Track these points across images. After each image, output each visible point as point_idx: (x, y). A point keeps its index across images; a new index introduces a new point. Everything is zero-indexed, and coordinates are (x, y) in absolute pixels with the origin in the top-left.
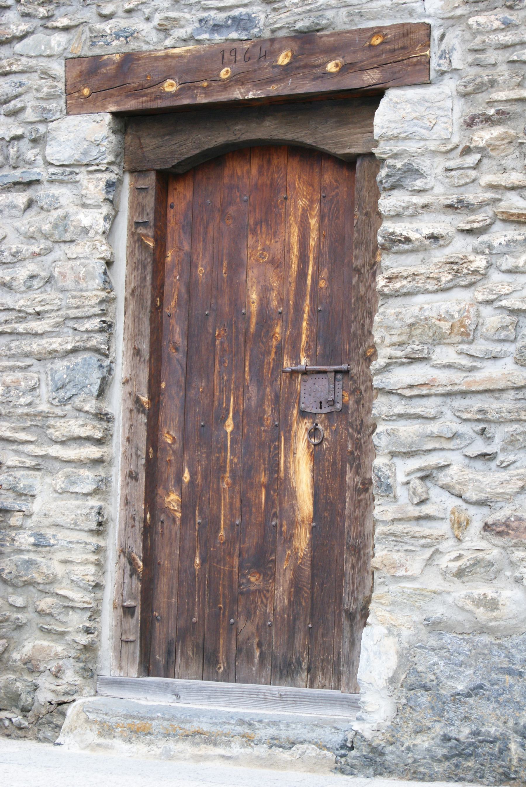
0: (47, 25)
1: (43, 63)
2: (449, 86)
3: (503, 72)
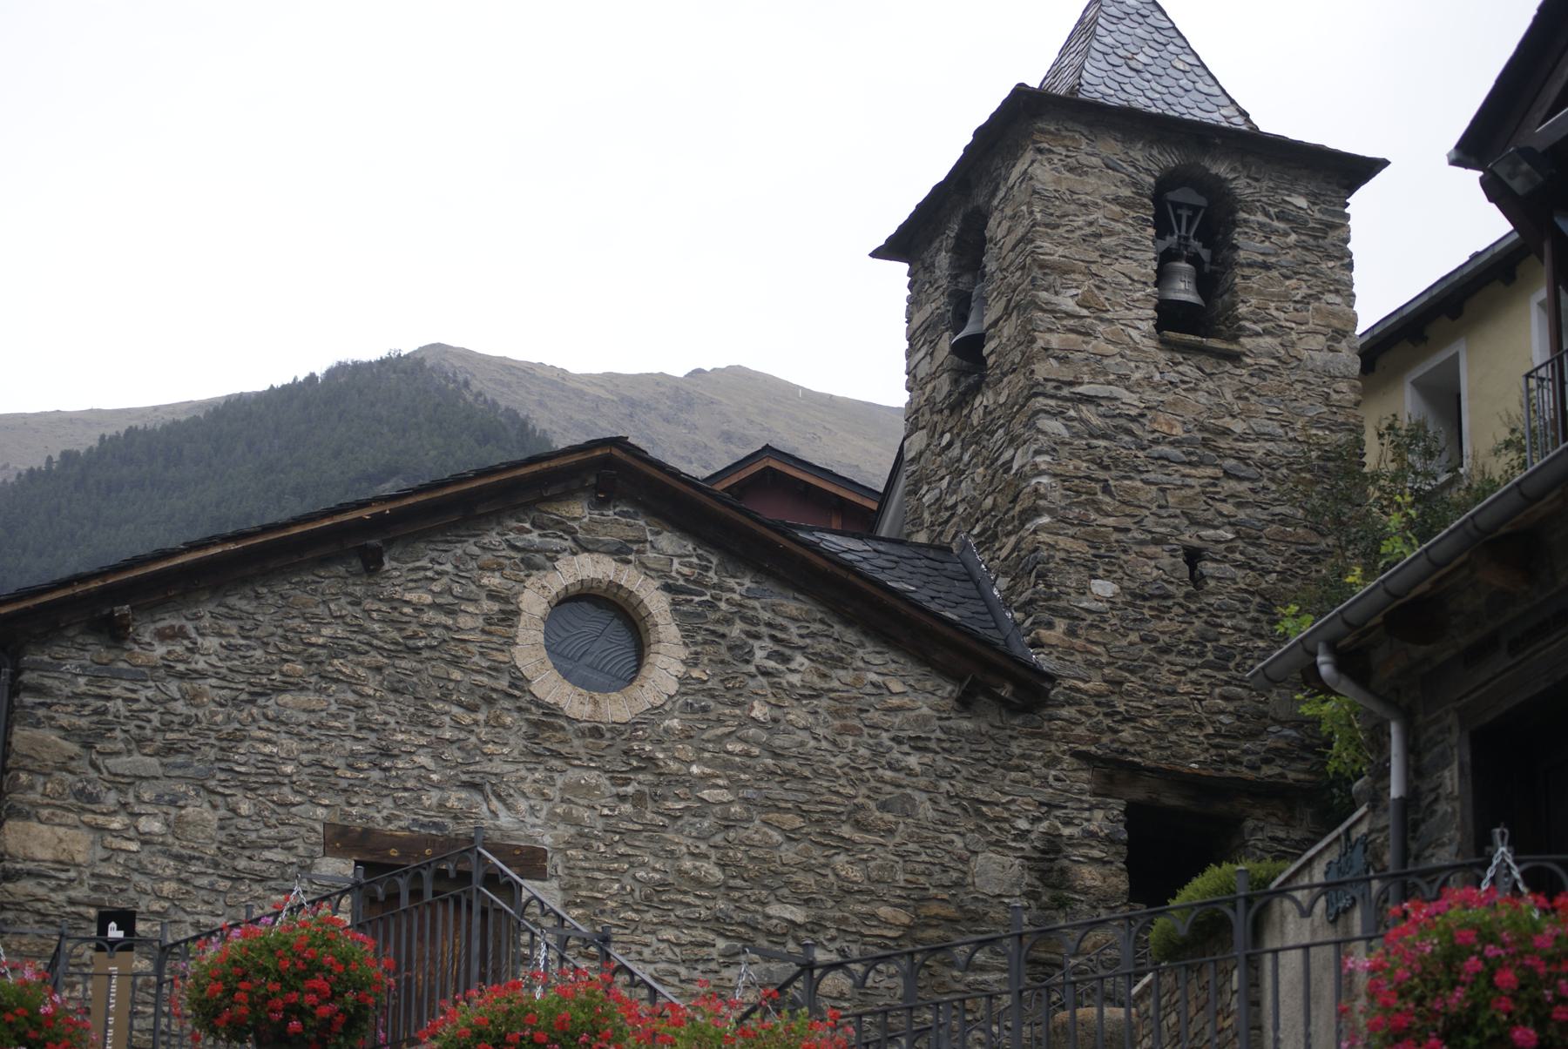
0: (312, 801)
1: (310, 823)
2: (555, 883)
3: (584, 883)
